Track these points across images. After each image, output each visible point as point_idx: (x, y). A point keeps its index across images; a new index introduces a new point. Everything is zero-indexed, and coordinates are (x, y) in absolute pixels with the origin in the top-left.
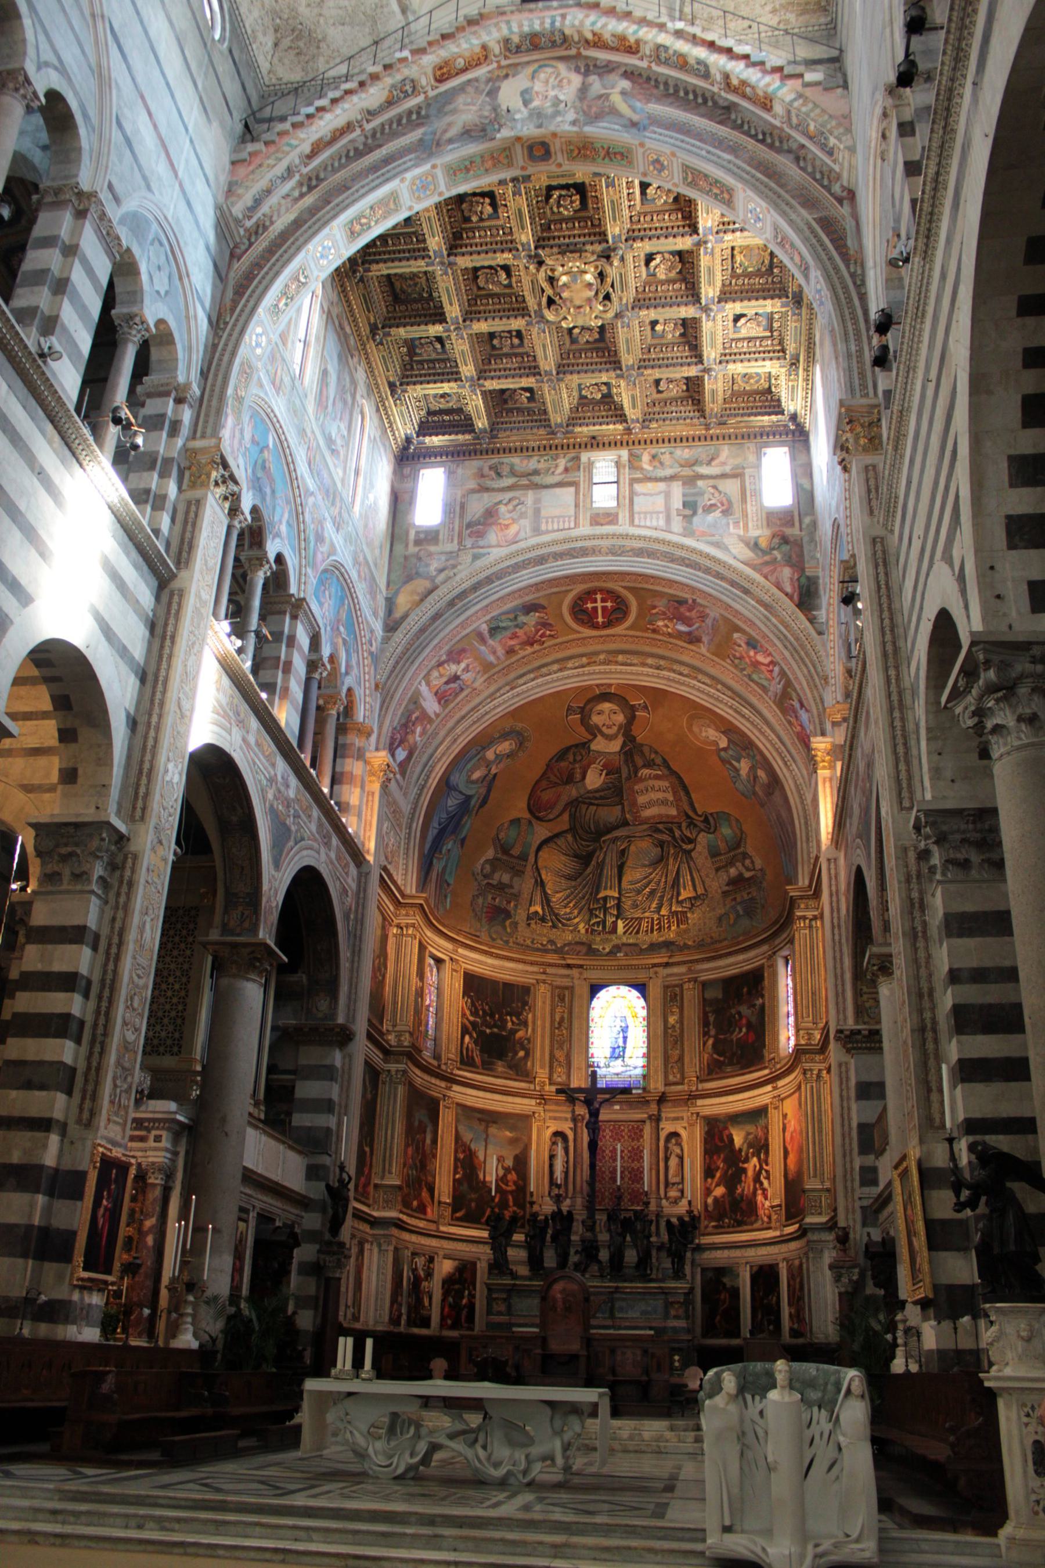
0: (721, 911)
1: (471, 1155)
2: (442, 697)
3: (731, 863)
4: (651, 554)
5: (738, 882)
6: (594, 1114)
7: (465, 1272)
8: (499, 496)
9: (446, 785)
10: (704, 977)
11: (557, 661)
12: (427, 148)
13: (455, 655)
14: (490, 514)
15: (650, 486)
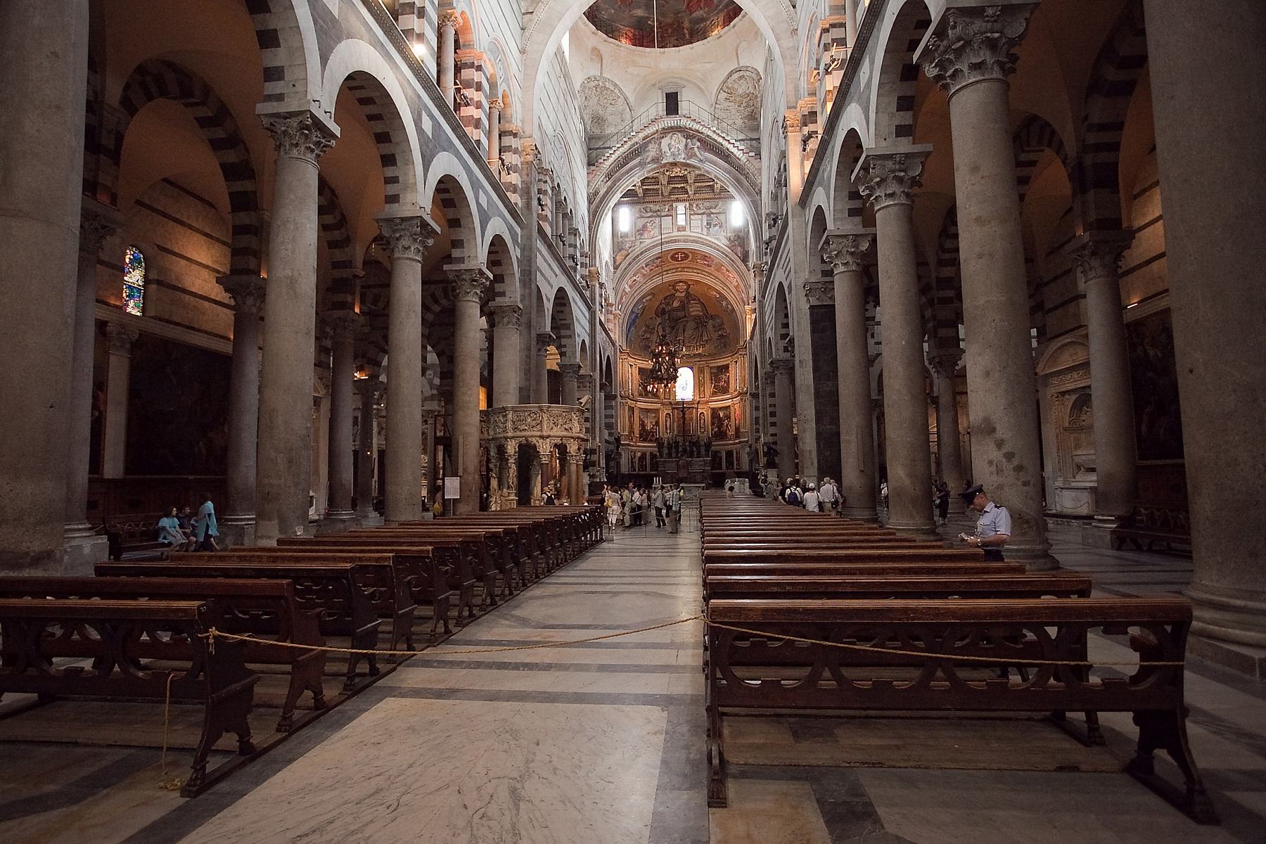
0: (716, 345)
1: (643, 422)
2: (630, 287)
3: (718, 331)
4: (697, 242)
5: (721, 336)
6: (684, 414)
7: (644, 454)
8: (647, 220)
9: (632, 312)
10: (711, 365)
11: (666, 271)
12: (642, 165)
13: (634, 275)
14: (644, 227)
15: (696, 216)
